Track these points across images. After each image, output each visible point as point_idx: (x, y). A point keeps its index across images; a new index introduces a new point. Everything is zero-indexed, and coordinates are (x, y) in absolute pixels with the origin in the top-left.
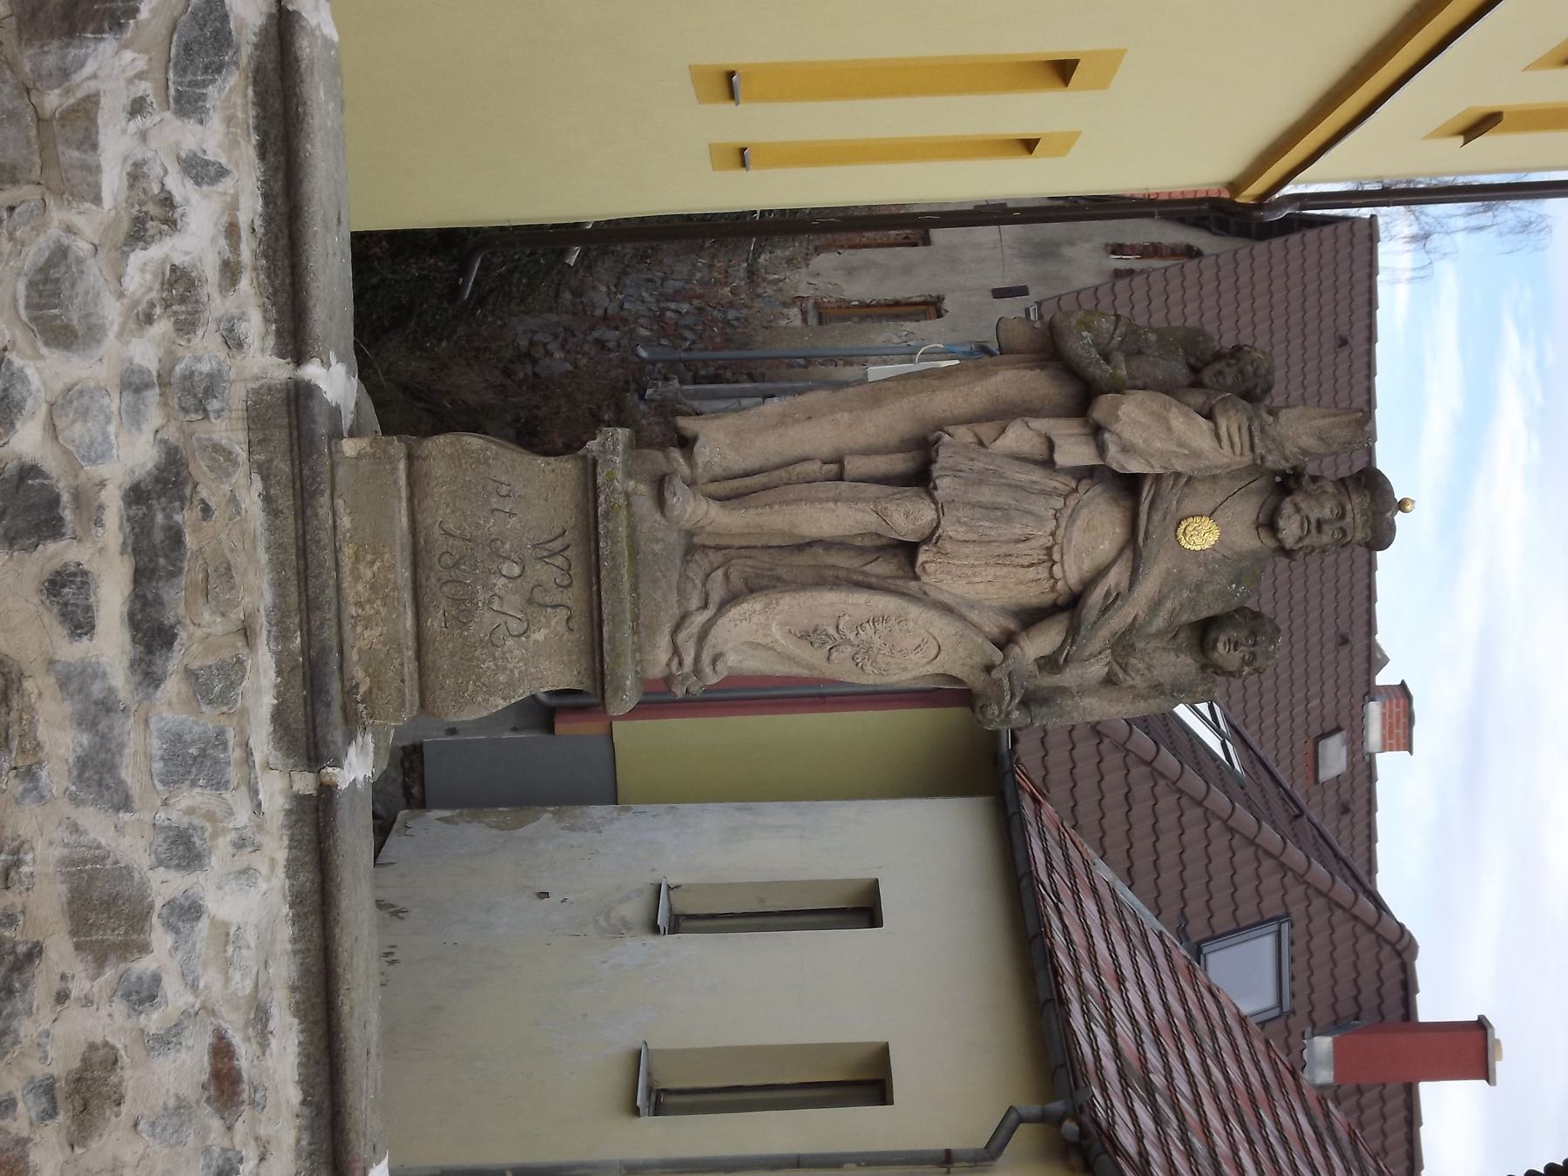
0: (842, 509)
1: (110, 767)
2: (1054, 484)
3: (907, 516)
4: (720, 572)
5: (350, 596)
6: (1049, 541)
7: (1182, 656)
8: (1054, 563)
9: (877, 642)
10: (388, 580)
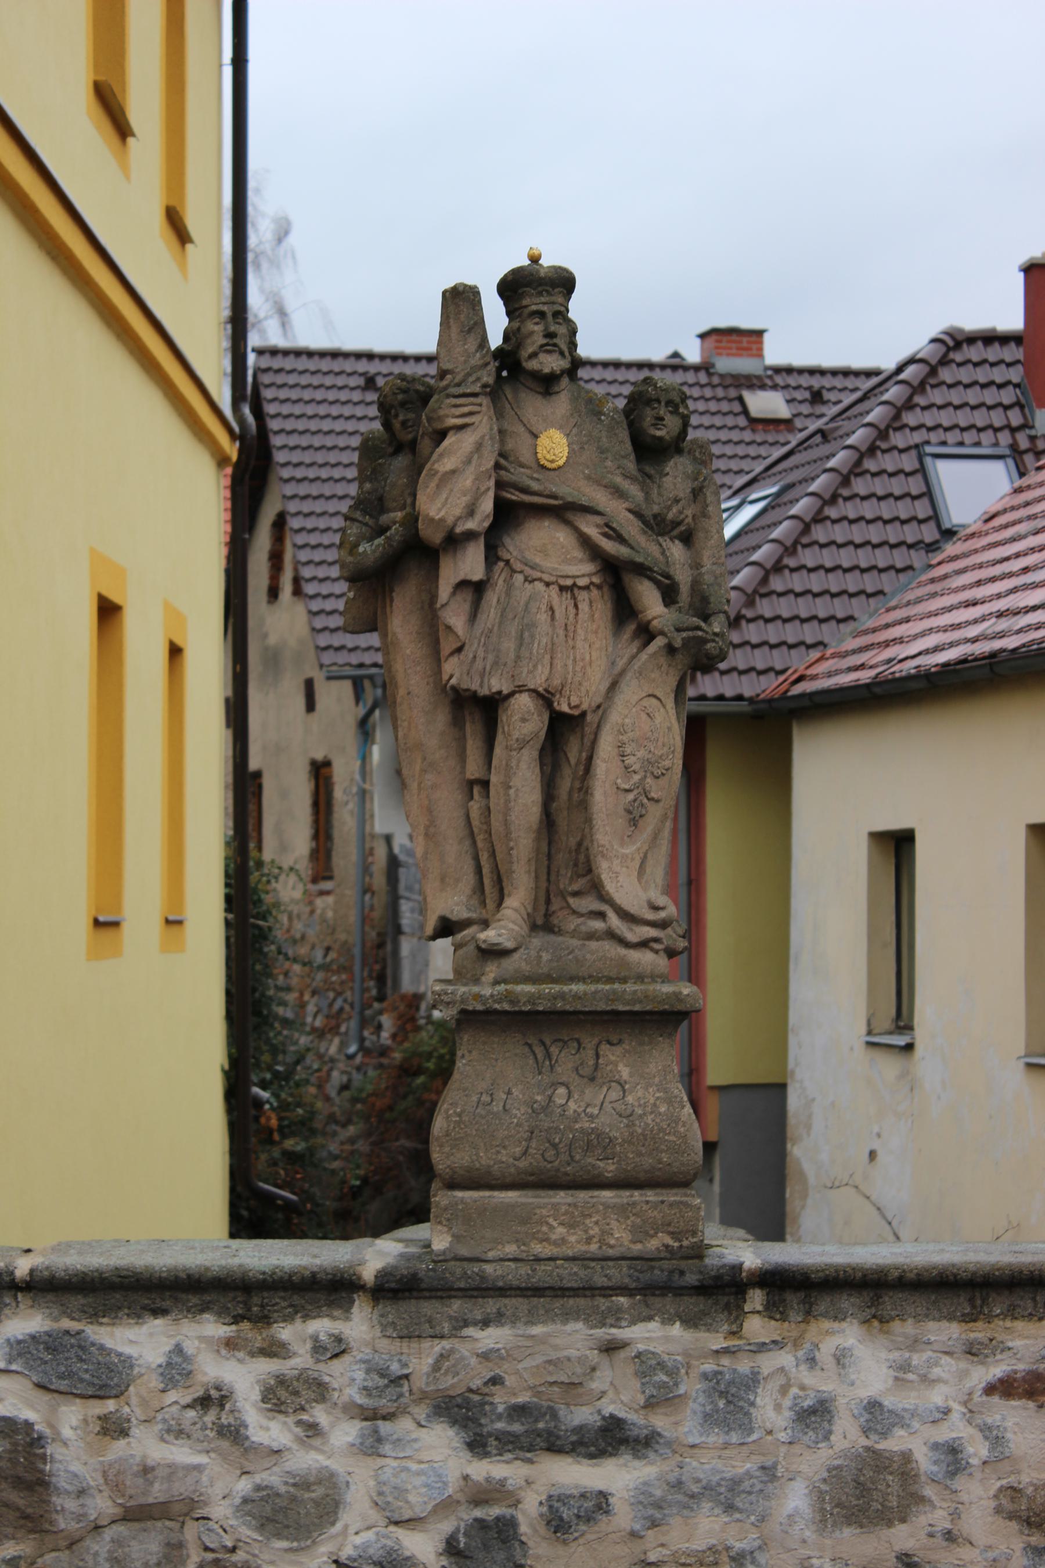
0: (516, 782)
1: (735, 1484)
2: (500, 582)
3: (523, 719)
4: (571, 900)
6: (554, 590)
7: (668, 469)
8: (574, 585)
10: (566, 1213)
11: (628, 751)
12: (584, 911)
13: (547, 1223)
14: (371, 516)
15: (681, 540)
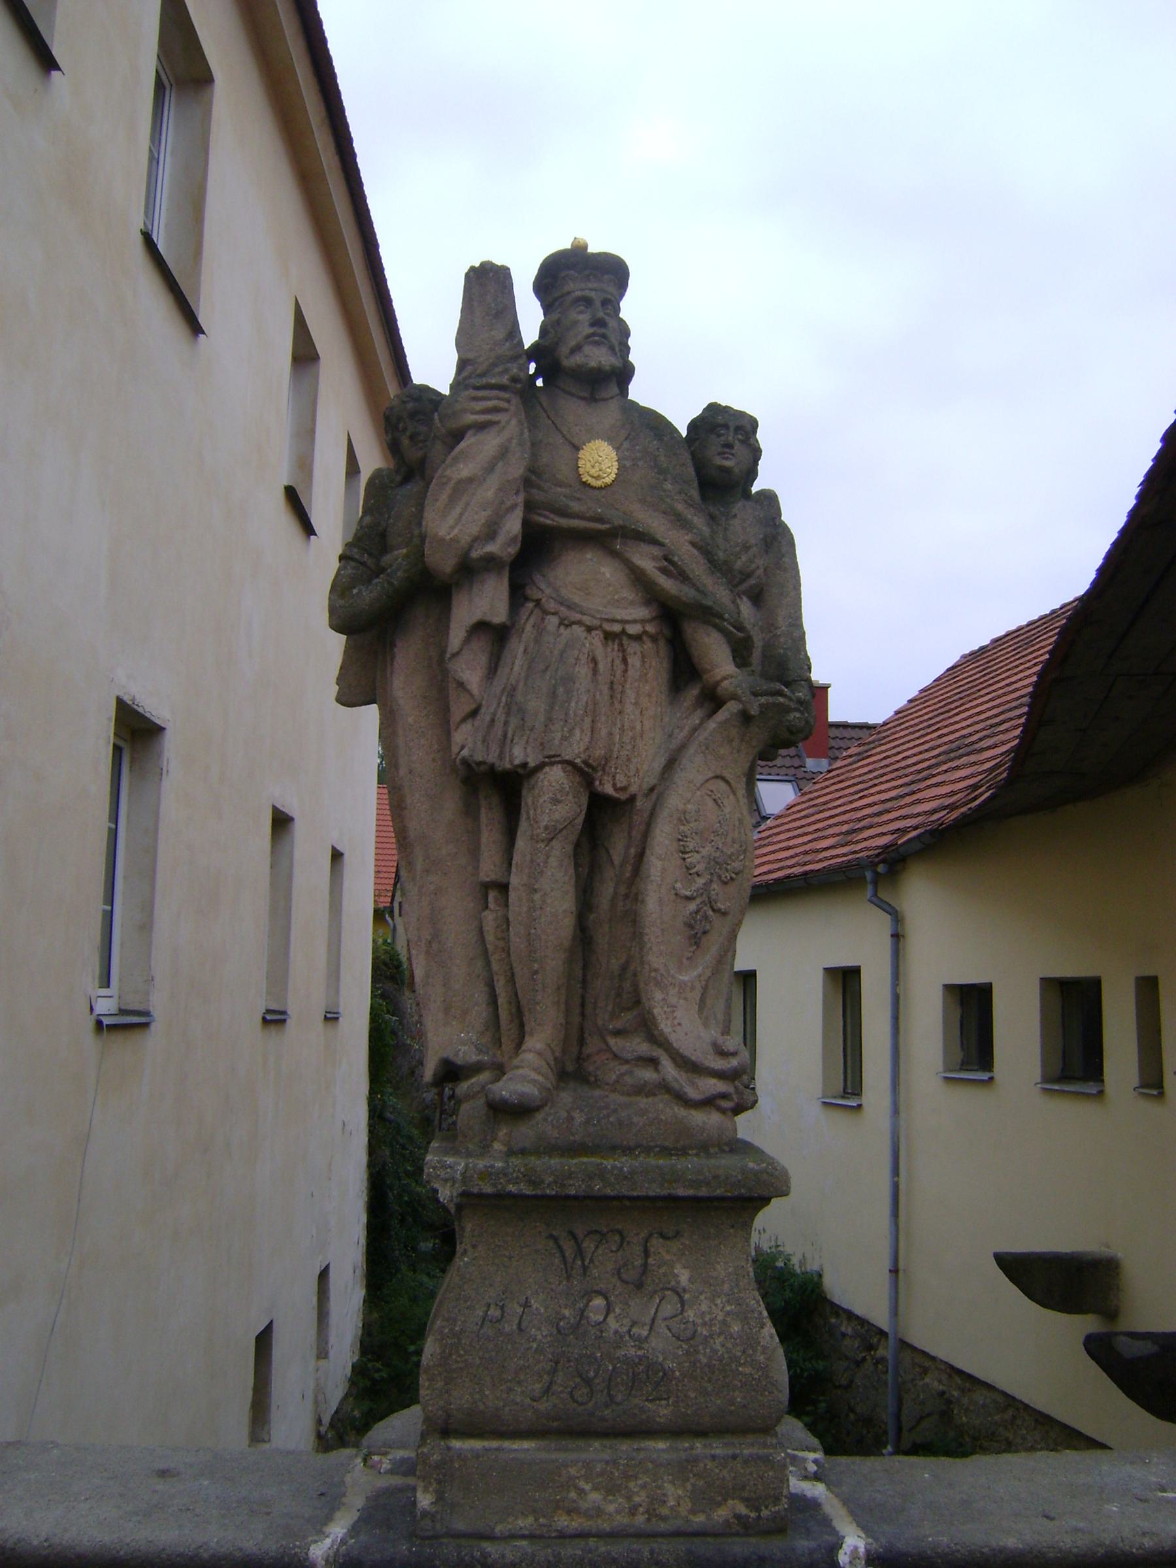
2: (528, 628)
3: (553, 801)
4: (612, 1041)
5: (622, 1520)
6: (597, 636)
7: (735, 511)
8: (624, 632)
9: (707, 850)
10: (601, 1474)
11: (691, 846)
12: (629, 1056)
13: (576, 1487)
14: (370, 554)
15: (750, 598)
